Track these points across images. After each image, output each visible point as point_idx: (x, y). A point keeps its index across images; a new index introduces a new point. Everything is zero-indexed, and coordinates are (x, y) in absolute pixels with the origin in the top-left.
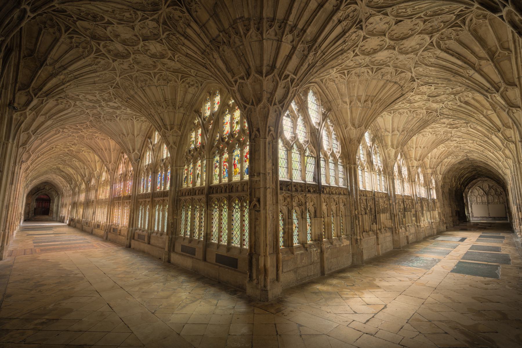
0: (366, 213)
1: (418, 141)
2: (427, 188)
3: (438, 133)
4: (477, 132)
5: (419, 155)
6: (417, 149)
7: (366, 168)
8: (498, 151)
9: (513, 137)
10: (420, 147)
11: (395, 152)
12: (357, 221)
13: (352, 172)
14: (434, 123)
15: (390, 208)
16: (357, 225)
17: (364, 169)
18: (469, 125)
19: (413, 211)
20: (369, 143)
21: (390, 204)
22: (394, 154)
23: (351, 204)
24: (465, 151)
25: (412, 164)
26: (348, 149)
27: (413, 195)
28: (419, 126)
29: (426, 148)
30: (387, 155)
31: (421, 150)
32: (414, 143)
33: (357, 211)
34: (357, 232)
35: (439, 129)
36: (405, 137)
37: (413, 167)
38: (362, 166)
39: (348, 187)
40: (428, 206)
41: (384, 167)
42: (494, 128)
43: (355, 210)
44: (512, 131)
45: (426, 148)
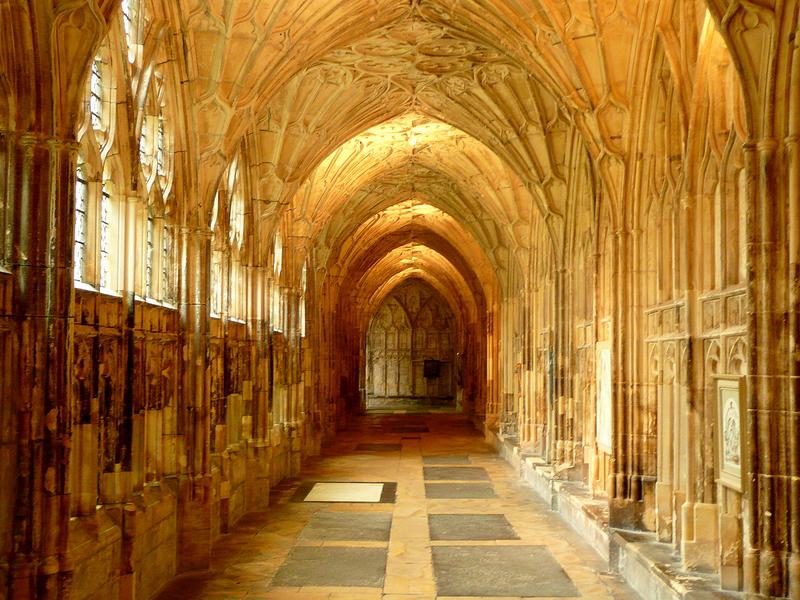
0: (86, 418)
1: (303, 94)
2: (289, 295)
3: (377, 77)
4: (491, 104)
5: (294, 159)
6: (294, 130)
7: (106, 176)
8: (533, 183)
9: (626, 136)
10: (306, 124)
11: (233, 121)
12: (51, 473)
13: (47, 184)
14: (383, 30)
15: (181, 382)
16: (46, 494)
17: (98, 178)
18: (476, 71)
19: (245, 390)
20: (135, 52)
21: (183, 364)
22: (225, 131)
23: (27, 373)
24: (419, 171)
25: (265, 188)
26: (40, 41)
27: (254, 322)
28: (339, 21)
29: (323, 132)
30: (195, 128)
31: (306, 136)
32: (289, 100)
33: (54, 413)
34: (45, 538)
35: (386, 62)
36: (282, 59)
37: (267, 202)
38: (93, 154)
39: (15, 268)
40: (286, 366)
41: (175, 183)
42: (583, 93)
43: (48, 405)
44: (628, 115)
45: (323, 132)
